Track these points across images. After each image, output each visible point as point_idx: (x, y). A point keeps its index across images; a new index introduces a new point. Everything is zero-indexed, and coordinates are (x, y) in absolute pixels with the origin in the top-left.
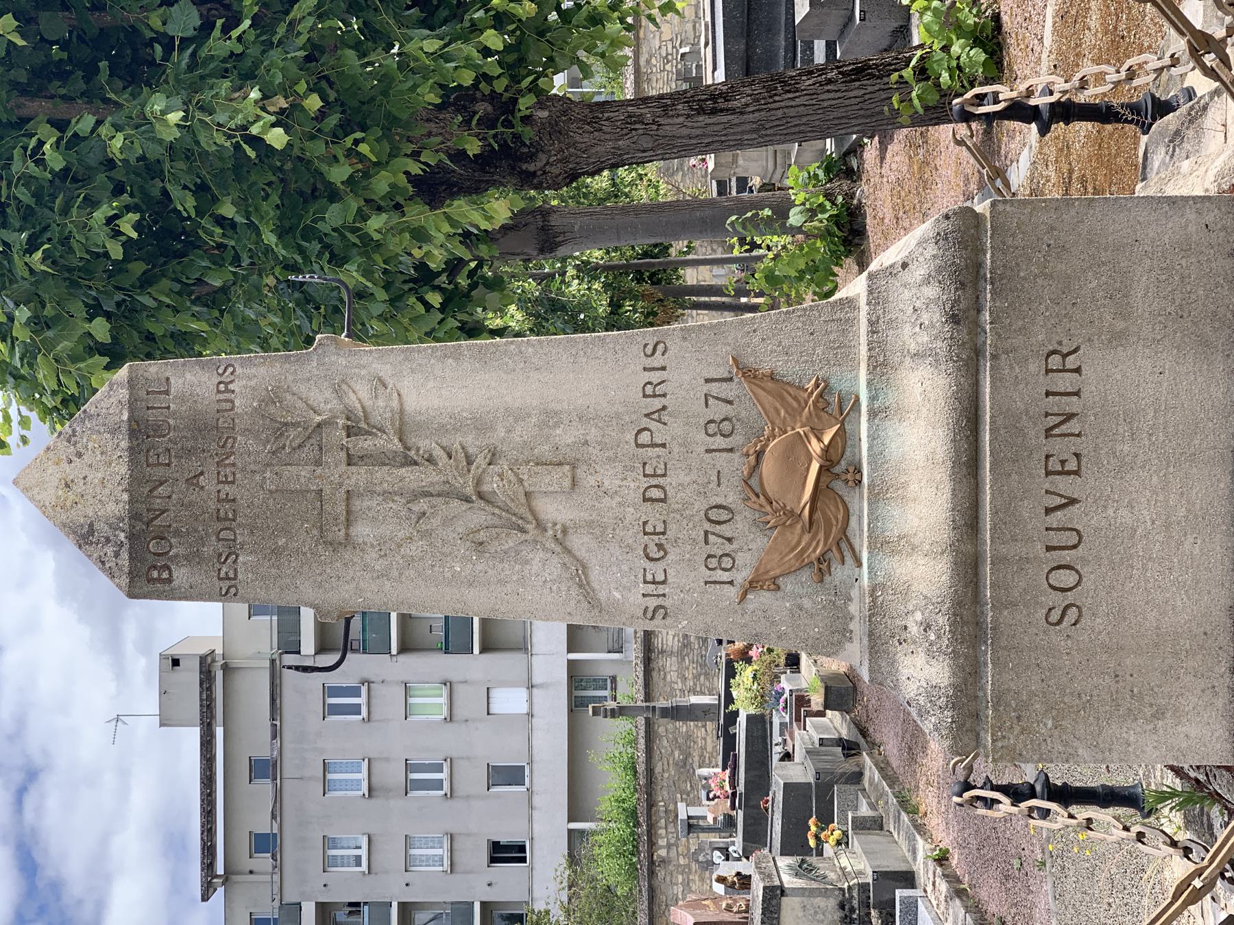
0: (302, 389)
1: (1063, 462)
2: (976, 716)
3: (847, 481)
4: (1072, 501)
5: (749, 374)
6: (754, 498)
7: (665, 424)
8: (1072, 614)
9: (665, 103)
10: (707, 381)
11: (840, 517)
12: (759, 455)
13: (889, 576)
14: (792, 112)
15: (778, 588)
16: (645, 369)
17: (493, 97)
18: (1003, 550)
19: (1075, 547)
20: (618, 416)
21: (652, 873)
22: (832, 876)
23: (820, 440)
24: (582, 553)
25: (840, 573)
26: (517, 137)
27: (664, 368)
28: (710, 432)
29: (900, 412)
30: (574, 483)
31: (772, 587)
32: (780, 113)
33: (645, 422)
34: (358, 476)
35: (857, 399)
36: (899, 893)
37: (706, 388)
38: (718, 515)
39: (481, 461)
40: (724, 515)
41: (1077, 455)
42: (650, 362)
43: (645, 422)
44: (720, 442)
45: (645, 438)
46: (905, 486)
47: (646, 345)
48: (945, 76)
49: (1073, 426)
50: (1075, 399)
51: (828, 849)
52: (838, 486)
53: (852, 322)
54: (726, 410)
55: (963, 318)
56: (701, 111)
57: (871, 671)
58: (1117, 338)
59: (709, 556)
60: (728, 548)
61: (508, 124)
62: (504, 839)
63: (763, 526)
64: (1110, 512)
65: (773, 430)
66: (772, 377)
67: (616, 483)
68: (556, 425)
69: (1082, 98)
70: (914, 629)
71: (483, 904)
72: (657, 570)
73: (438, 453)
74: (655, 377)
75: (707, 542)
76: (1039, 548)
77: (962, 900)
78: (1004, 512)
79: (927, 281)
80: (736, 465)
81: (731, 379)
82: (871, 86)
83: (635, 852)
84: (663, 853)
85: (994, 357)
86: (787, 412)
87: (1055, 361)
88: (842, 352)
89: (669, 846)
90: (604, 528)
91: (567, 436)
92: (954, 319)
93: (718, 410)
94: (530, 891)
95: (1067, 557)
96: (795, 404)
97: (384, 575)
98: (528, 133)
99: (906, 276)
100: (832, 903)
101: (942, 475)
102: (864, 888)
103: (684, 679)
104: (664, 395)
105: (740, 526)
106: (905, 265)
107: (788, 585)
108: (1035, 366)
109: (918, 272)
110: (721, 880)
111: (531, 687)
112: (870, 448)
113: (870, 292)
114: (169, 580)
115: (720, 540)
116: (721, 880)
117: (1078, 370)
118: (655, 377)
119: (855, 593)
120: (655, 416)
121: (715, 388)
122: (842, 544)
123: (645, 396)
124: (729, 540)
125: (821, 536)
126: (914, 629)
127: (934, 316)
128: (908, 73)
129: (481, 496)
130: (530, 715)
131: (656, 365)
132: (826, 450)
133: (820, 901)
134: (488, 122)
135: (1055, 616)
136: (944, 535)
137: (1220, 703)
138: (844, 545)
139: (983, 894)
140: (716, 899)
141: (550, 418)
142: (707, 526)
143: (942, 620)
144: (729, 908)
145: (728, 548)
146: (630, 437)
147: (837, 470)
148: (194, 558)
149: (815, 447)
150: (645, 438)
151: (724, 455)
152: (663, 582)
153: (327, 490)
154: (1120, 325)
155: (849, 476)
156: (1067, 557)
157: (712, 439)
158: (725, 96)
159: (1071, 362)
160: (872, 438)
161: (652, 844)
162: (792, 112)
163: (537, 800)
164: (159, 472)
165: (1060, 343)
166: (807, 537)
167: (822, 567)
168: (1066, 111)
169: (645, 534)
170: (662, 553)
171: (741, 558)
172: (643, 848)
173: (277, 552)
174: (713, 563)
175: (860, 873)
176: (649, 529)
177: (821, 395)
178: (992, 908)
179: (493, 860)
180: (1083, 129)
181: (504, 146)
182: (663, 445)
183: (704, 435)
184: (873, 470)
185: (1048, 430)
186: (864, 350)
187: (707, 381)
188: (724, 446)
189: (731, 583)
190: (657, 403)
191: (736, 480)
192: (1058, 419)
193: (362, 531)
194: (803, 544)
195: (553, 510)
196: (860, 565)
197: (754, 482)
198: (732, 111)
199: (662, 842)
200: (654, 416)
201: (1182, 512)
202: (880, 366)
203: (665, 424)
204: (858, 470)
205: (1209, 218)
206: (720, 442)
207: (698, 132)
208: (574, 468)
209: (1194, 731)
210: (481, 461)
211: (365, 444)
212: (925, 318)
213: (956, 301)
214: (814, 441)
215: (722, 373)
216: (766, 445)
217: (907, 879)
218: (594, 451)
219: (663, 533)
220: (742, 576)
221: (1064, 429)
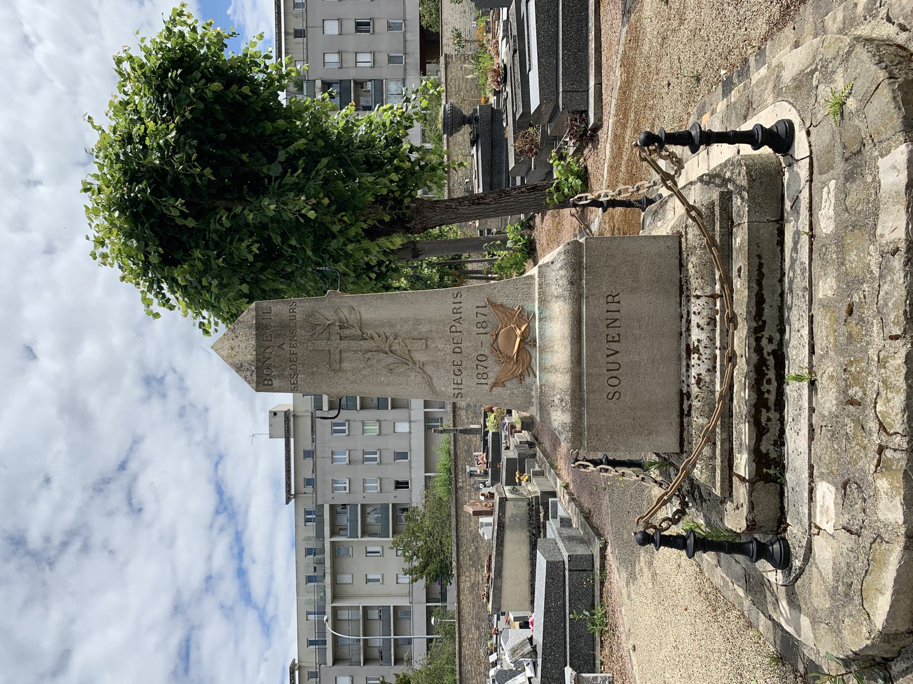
0: (322, 311)
2: (581, 434)
4: (617, 352)
5: (493, 305)
8: (617, 395)
9: (460, 201)
12: (497, 335)
17: (394, 199)
18: (591, 371)
21: (456, 492)
22: (525, 493)
24: (430, 373)
25: (528, 380)
26: (404, 214)
29: (551, 319)
33: (454, 323)
34: (344, 344)
36: (550, 500)
37: (476, 310)
38: (481, 358)
39: (391, 338)
43: (454, 323)
45: (453, 329)
48: (566, 190)
49: (617, 324)
51: (523, 483)
52: (527, 347)
53: (532, 284)
55: (575, 282)
56: (474, 204)
58: (633, 290)
60: (485, 371)
61: (400, 209)
62: (400, 480)
63: (499, 362)
66: (502, 305)
67: (443, 347)
68: (420, 325)
69: (618, 198)
70: (557, 401)
71: (393, 505)
73: (375, 335)
74: (457, 306)
76: (605, 370)
78: (591, 356)
79: (561, 268)
80: (488, 339)
82: (538, 194)
83: (450, 484)
84: (461, 484)
85: (587, 297)
88: (529, 296)
89: (463, 482)
90: (438, 363)
91: (424, 329)
92: (571, 283)
93: (481, 318)
94: (411, 499)
95: (615, 373)
97: (354, 382)
98: (408, 212)
99: (553, 267)
100: (525, 503)
101: (567, 342)
102: (537, 497)
103: (468, 419)
105: (490, 362)
106: (552, 263)
107: (508, 384)
108: (603, 301)
109: (558, 265)
110: (483, 495)
111: (410, 422)
114: (272, 385)
117: (619, 302)
118: (457, 306)
119: (534, 388)
121: (480, 310)
126: (557, 401)
127: (564, 282)
128: (552, 189)
129: (391, 351)
130: (410, 432)
132: (522, 333)
133: (520, 503)
134: (392, 208)
135: (610, 396)
136: (568, 365)
139: (582, 500)
140: (481, 502)
141: (418, 321)
142: (477, 362)
143: (567, 398)
144: (486, 506)
145: (485, 371)
148: (281, 376)
149: (518, 332)
150: (453, 329)
153: (332, 350)
156: (615, 373)
158: (483, 198)
160: (540, 328)
161: (456, 481)
163: (413, 465)
164: (267, 343)
167: (521, 378)
168: (613, 203)
173: (313, 373)
174: (480, 376)
175: (535, 492)
178: (586, 505)
179: (396, 488)
180: (619, 210)
181: (399, 217)
184: (540, 341)
190: (458, 316)
191: (488, 345)
193: (346, 365)
195: (419, 357)
197: (495, 346)
198: (486, 204)
201: (658, 356)
202: (543, 301)
205: (669, 244)
209: (663, 440)
210: (391, 338)
211: (347, 332)
212: (560, 282)
213: (572, 276)
215: (483, 304)
217: (554, 494)
218: (434, 334)
220: (490, 381)
221: (613, 325)
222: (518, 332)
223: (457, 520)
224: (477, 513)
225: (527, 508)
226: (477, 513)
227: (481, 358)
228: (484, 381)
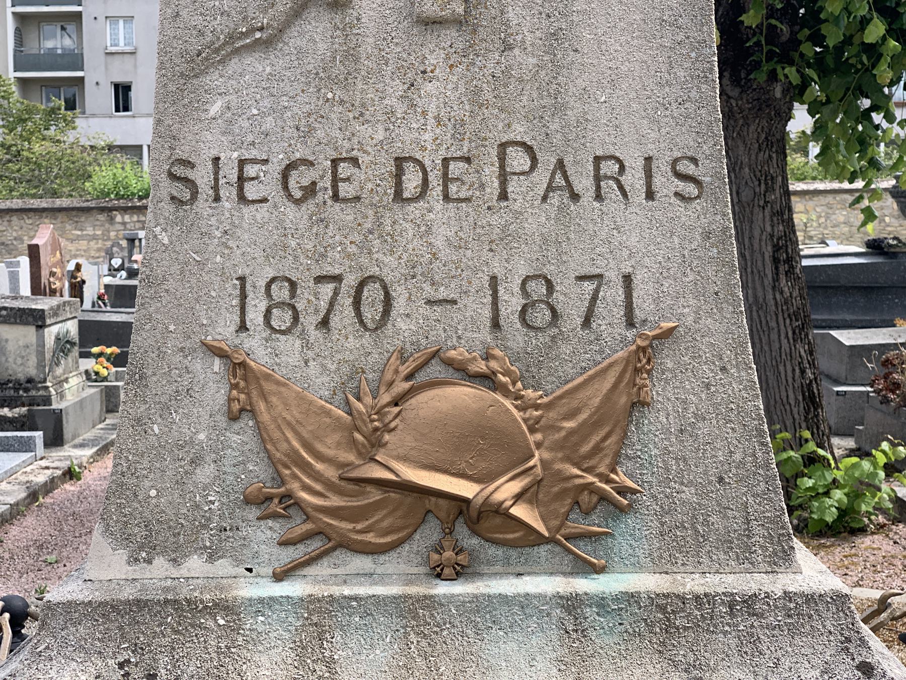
3: (439, 549)
5: (642, 360)
6: (405, 370)
7: (545, 198)
9: (784, 215)
10: (628, 279)
11: (370, 537)
12: (487, 380)
13: (254, 640)
14: (774, 336)
15: (233, 418)
16: (648, 160)
17: (795, 43)
20: (559, 109)
21: (102, 210)
22: (59, 371)
23: (518, 498)
24: (294, 40)
25: (263, 537)
26: (757, 65)
27: (650, 195)
28: (532, 285)
30: (430, 23)
31: (236, 407)
32: (773, 324)
33: (547, 161)
35: (599, 570)
36: (38, 435)
37: (613, 276)
38: (372, 302)
40: (371, 314)
42: (662, 168)
43: (547, 161)
44: (512, 303)
45: (518, 160)
47: (694, 161)
48: (810, 483)
51: (88, 364)
53: (745, 557)
54: (573, 315)
56: (777, 248)
57: (69, 606)
59: (293, 285)
60: (309, 321)
61: (770, 56)
62: (133, 94)
63: (350, 387)
65: (537, 407)
71: (82, 79)
72: (264, 184)
74: (634, 179)
75: (319, 279)
77: (25, 498)
80: (468, 336)
81: (630, 324)
82: (798, 411)
83: (119, 197)
84: (119, 218)
86: (572, 432)
88: (682, 542)
89: (124, 223)
90: (346, 82)
93: (572, 300)
94: (93, 115)
96: (586, 448)
98: (761, 77)
100: (32, 372)
102: (47, 400)
104: (599, 197)
105: (350, 343)
107: (240, 437)
110: (78, 267)
112: (504, 599)
113: (810, 599)
115: (323, 305)
116: (78, 267)
118: (634, 179)
119: (223, 567)
120: (559, 180)
122: (321, 540)
123: (598, 160)
124: (324, 323)
125: (335, 501)
128: (811, 446)
131: (658, 181)
132: (499, 511)
133: (33, 361)
134: (772, 34)
138: (316, 545)
139: (29, 520)
140: (62, 263)
142: (351, 280)
144: (52, 274)
145: (309, 321)
146: (519, 132)
147: (461, 530)
149: (505, 490)
150: (518, 160)
151: (487, 313)
152: (242, 198)
155: (448, 554)
157: (517, 289)
158: (790, 272)
161: (125, 210)
162: (774, 336)
166: (331, 473)
167: (272, 502)
169: (335, 162)
170: (298, 194)
171: (290, 345)
172: (122, 203)
175: (61, 395)
176: (344, 170)
177: (604, 498)
178: (14, 531)
179: (117, 86)
181: (748, 52)
182: (503, 196)
183: (524, 271)
186: (693, 583)
187: (628, 279)
188: (503, 312)
189: (243, 327)
190: (584, 183)
191: (438, 334)
194: (319, 466)
196: (279, 577)
197: (435, 370)
198: (776, 279)
199: (127, 218)
200: (558, 176)
203: (545, 198)
204: (460, 573)
206: (512, 303)
207: (756, 246)
208: (458, 22)
214: (516, 487)
215: (643, 307)
216: (506, 393)
217: (55, 440)
218: (492, 63)
219: (336, 197)
222: (505, 490)
223: (44, 210)
224: (34, 253)
225: (21, 377)
226: (34, 253)
227: (372, 302)
228: (255, 316)
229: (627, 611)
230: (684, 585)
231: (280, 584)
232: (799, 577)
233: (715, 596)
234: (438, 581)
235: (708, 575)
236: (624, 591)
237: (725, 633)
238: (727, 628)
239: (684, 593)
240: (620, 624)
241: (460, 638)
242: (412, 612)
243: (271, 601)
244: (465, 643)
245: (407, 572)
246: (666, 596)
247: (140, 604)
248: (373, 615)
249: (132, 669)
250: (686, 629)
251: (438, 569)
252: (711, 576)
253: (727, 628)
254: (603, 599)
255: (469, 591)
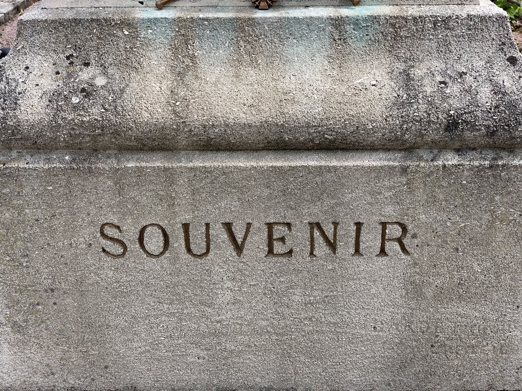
1: (282, 240)
4: (239, 248)
13: (147, 44)
18: (182, 181)
19: (189, 250)
41: (290, 252)
46: (254, 64)
50: (352, 250)
57: (34, 22)
58: (415, 289)
64: (229, 284)
70: (85, 75)
76: (187, 217)
77: (12, 11)
78: (226, 180)
79: (498, 90)
87: (395, 231)
92: (452, 125)
95: (178, 243)
99: (500, 62)
101: (268, 112)
108: (390, 212)
112: (297, 20)
113: (483, 19)
117: (383, 252)
127: (455, 100)
135: (110, 232)
136: (196, 117)
137: (38, 379)
143: (96, 112)
154: (429, 292)
159: (393, 247)
165: (414, 236)
184: (271, 23)
185: (318, 225)
192: (330, 235)
196: (160, 7)
201: (230, 346)
212: (453, 89)
213: (473, 127)
229: (371, 27)
230: (407, 12)
231: (161, 11)
232: (477, 7)
233: (425, 18)
234: (257, 10)
235: (422, 6)
236: (370, 15)
237: (430, 40)
238: (431, 37)
239: (407, 16)
240: (367, 35)
241: (270, 44)
242: (241, 28)
243: (155, 21)
244: (273, 47)
245: (238, 5)
246: (396, 18)
247: (76, 22)
248: (217, 30)
249: (75, 60)
250: (406, 37)
251: (257, 3)
252: (424, 6)
253: (431, 37)
254: (357, 20)
255: (276, 16)
